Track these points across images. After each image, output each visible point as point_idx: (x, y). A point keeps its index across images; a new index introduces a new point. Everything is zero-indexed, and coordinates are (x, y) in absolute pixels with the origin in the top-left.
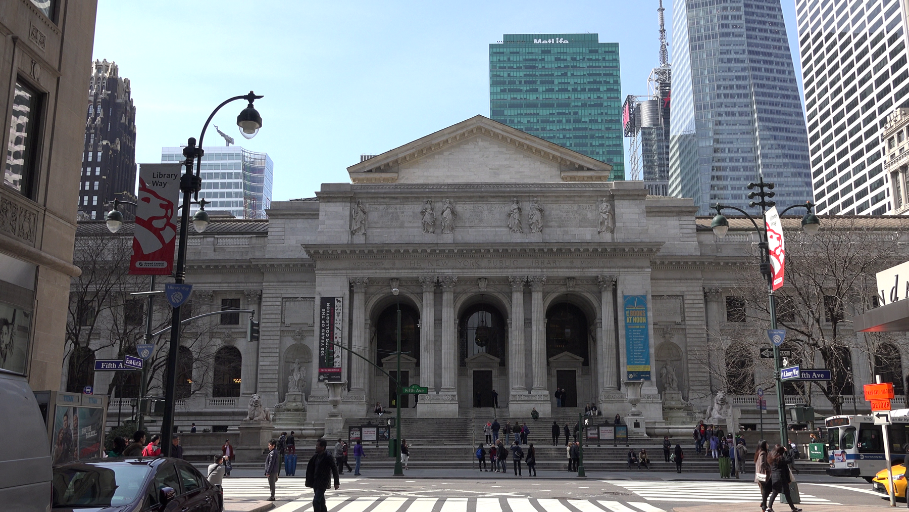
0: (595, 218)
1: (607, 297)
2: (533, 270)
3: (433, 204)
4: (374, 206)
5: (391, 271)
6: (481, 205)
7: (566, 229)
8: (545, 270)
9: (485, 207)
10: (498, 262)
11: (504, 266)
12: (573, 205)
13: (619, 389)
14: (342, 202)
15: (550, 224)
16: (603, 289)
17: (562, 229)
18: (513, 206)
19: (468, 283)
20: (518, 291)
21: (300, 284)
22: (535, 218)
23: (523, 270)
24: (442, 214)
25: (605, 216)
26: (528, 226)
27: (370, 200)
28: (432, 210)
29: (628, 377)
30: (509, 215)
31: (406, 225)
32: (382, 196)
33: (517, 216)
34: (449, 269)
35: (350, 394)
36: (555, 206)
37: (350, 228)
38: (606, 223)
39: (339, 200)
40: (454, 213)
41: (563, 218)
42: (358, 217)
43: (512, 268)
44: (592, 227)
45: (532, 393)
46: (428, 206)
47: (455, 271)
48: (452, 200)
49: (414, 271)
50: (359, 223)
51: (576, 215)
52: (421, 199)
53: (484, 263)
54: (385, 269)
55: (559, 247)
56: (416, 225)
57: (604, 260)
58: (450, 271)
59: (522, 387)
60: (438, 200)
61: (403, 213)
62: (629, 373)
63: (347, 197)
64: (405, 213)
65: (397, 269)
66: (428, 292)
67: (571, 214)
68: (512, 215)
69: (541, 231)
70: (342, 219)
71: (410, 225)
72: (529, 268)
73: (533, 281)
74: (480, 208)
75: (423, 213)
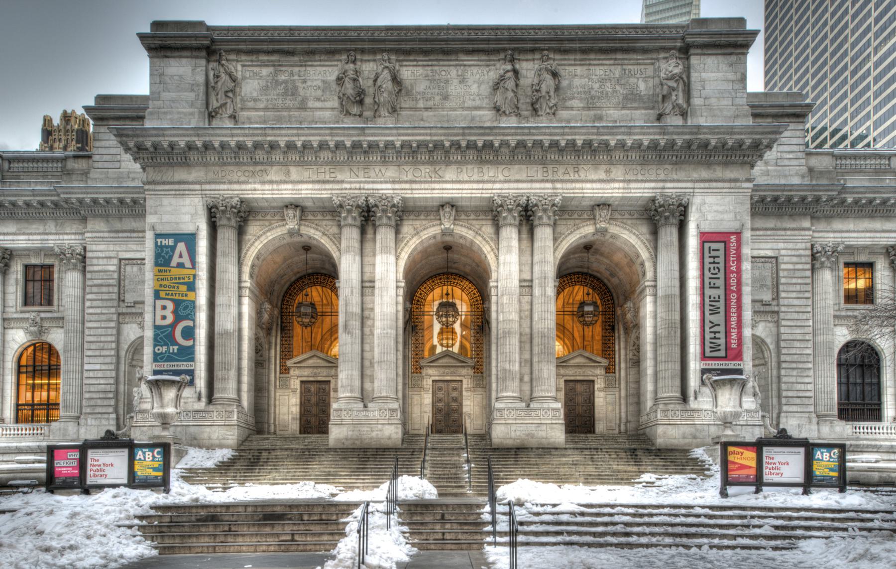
0: (651, 93)
2: (537, 185)
3: (359, 63)
4: (251, 69)
5: (283, 186)
6: (444, 68)
7: (599, 112)
8: (559, 185)
9: (453, 72)
10: (476, 170)
11: (486, 178)
12: (612, 68)
13: (684, 398)
14: (191, 57)
15: (569, 103)
16: (663, 221)
17: (592, 113)
18: (503, 67)
20: (511, 225)
22: (544, 88)
23: (521, 185)
24: (375, 81)
25: (672, 84)
26: (530, 108)
27: (243, 58)
28: (356, 72)
30: (496, 87)
31: (311, 104)
33: (510, 84)
34: (386, 182)
35: (211, 407)
36: (579, 70)
37: (207, 107)
38: (674, 98)
39: (188, 54)
40: (396, 80)
41: (593, 93)
42: (220, 84)
43: (500, 182)
44: (646, 108)
45: (533, 405)
46: (352, 66)
47: (397, 186)
48: (393, 57)
50: (221, 95)
51: (618, 88)
52: (337, 57)
53: (450, 173)
54: (271, 182)
56: (329, 104)
57: (667, 166)
58: (389, 186)
59: (515, 395)
60: (366, 57)
61: (304, 82)
63: (198, 49)
64: (309, 83)
65: (293, 182)
66: (350, 225)
67: (608, 84)
69: (554, 114)
70: (192, 90)
71: (318, 104)
72: (532, 181)
73: (536, 205)
74: (443, 73)
75: (340, 80)
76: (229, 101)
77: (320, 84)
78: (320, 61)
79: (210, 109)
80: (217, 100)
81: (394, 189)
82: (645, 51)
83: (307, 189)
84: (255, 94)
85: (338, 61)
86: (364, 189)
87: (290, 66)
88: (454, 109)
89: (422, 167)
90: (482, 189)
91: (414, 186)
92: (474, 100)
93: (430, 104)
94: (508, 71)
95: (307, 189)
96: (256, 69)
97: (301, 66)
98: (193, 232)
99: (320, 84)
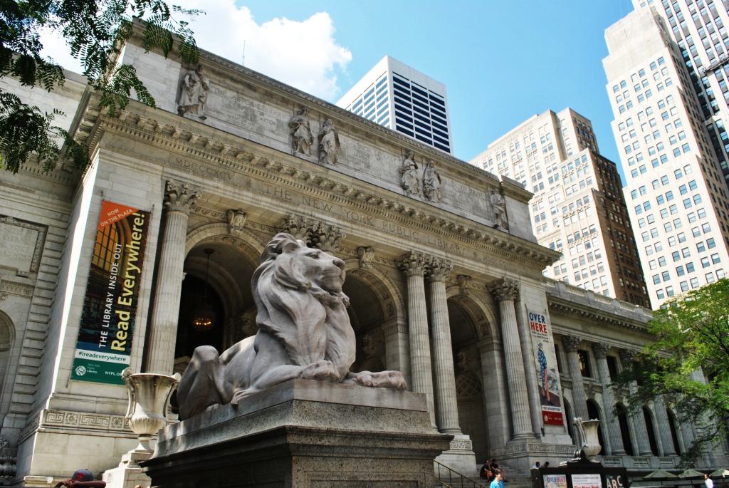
1: (508, 309)
4: (217, 86)
8: (449, 255)
9: (373, 151)
19: (344, 252)
21: (18, 191)
29: (544, 420)
32: (235, 76)
36: (448, 181)
37: (178, 101)
40: (337, 140)
44: (486, 218)
49: (282, 204)
51: (469, 200)
52: (290, 106)
55: (471, 228)
57: (504, 260)
62: (544, 413)
64: (266, 117)
68: (408, 172)
70: (164, 83)
71: (271, 135)
74: (366, 149)
76: (200, 104)
77: (275, 121)
78: (277, 104)
79: (181, 105)
80: (190, 100)
81: (338, 224)
82: (481, 182)
83: (266, 202)
84: (219, 108)
85: (290, 109)
86: (314, 217)
87: (252, 98)
88: (375, 177)
89: (359, 214)
90: (402, 243)
91: (354, 226)
92: (387, 175)
93: (357, 167)
94: (412, 165)
95: (266, 202)
96: (221, 89)
97: (261, 102)
98: (148, 210)
99: (275, 121)
